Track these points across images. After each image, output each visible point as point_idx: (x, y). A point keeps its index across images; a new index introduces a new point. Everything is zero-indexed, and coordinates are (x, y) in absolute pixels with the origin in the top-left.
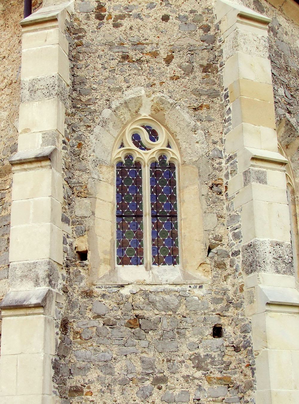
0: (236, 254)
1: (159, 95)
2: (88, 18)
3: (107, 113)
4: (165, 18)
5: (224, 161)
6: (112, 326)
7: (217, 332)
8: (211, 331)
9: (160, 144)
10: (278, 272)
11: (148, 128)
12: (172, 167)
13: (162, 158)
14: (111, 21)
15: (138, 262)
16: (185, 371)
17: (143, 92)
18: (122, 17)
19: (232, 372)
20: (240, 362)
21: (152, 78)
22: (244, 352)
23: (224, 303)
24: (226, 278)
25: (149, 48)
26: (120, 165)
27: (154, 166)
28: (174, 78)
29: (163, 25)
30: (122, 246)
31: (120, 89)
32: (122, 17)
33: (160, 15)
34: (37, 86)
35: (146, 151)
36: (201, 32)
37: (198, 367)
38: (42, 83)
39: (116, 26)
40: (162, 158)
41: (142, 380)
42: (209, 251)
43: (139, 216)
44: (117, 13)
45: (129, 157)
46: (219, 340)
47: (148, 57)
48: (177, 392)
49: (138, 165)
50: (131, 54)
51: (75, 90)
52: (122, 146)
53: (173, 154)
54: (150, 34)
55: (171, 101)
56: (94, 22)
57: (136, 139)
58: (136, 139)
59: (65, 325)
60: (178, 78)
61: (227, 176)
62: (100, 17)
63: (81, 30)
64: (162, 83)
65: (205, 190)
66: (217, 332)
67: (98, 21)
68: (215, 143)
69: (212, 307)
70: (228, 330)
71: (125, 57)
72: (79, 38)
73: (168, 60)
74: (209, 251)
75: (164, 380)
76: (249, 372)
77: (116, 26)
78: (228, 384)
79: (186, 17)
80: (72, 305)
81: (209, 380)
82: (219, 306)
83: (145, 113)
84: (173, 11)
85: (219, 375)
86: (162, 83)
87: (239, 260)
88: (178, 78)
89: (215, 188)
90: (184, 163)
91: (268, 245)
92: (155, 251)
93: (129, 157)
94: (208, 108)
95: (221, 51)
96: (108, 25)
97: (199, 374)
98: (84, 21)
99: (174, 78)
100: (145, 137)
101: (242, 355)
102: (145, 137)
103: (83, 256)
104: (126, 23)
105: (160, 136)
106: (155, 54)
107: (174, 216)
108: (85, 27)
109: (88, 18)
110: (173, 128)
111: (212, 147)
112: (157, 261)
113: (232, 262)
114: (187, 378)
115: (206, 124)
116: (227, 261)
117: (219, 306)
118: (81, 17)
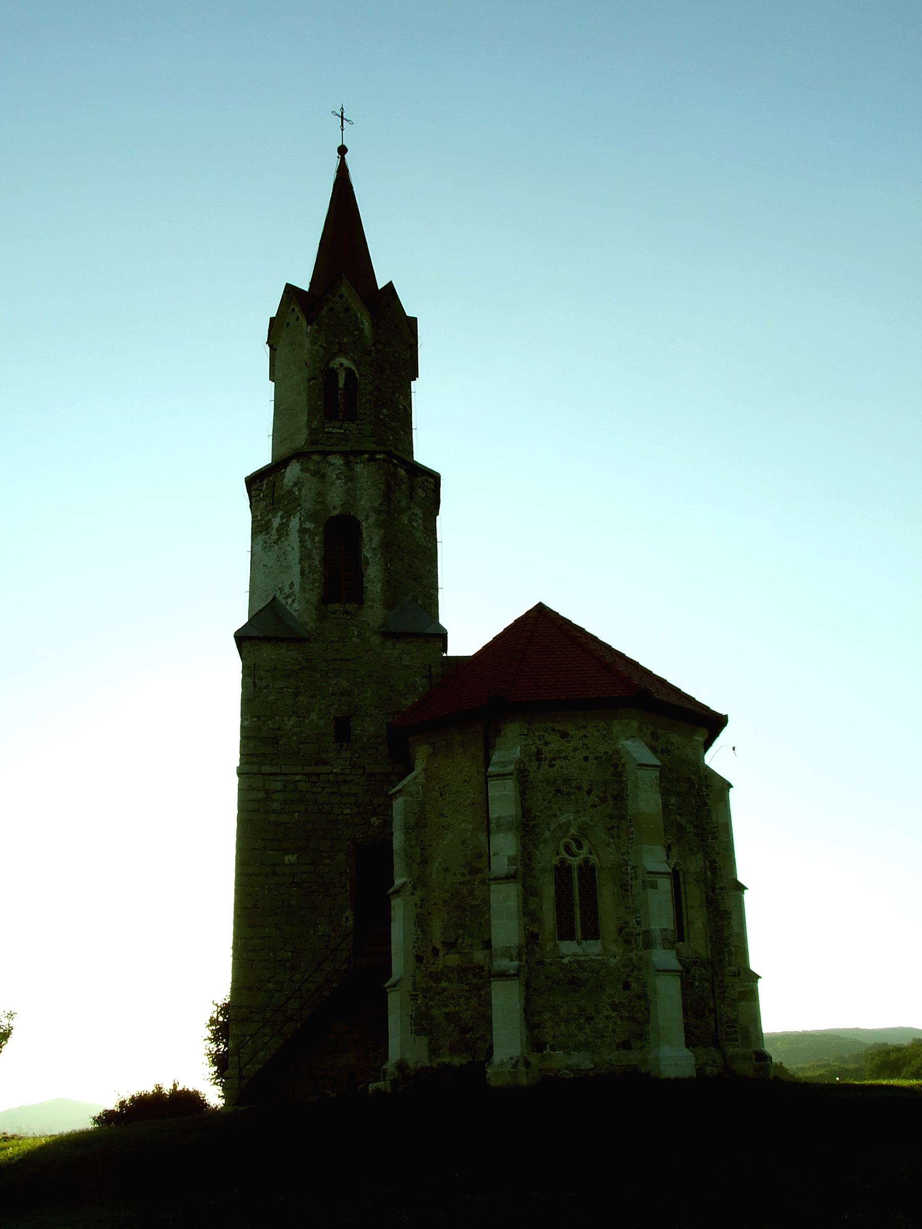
0: (638, 934)
2: (530, 761)
4: (586, 759)
7: (627, 986)
9: (585, 850)
10: (665, 949)
11: (576, 841)
13: (586, 861)
14: (547, 762)
15: (571, 937)
16: (605, 1013)
25: (574, 783)
28: (594, 806)
31: (555, 816)
33: (581, 757)
36: (612, 768)
37: (615, 1010)
39: (551, 766)
42: (621, 931)
44: (551, 756)
46: (627, 992)
47: (574, 790)
48: (601, 1026)
50: (563, 788)
53: (594, 859)
56: (535, 764)
57: (567, 848)
58: (567, 848)
61: (631, 879)
62: (539, 760)
63: (526, 770)
68: (623, 854)
69: (622, 970)
71: (559, 791)
72: (525, 776)
73: (589, 792)
74: (621, 931)
75: (592, 1018)
76: (646, 1013)
77: (551, 766)
78: (632, 1019)
79: (601, 758)
81: (621, 1018)
83: (573, 831)
87: (640, 939)
88: (596, 806)
93: (563, 861)
94: (618, 827)
96: (545, 765)
97: (614, 1014)
98: (528, 764)
99: (594, 806)
106: (579, 788)
109: (530, 761)
112: (585, 937)
114: (607, 1017)
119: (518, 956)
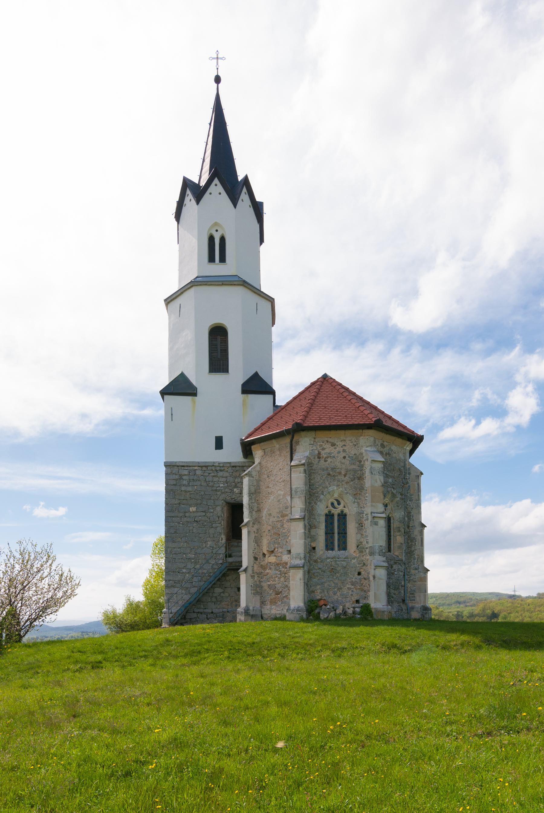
0: (367, 548)
1: (341, 489)
2: (314, 458)
3: (322, 497)
4: (344, 457)
5: (364, 515)
6: (324, 572)
7: (359, 574)
8: (357, 573)
9: (342, 505)
10: (380, 555)
11: (337, 500)
12: (346, 515)
13: (342, 511)
14: (323, 459)
15: (332, 549)
16: (348, 586)
17: (335, 488)
18: (327, 457)
19: (202, 606)
20: (366, 583)
21: (339, 483)
22: (367, 580)
23: (362, 565)
24: (363, 556)
25: (338, 470)
26: (326, 515)
27: (339, 515)
28: (347, 483)
29: (343, 461)
30: (327, 546)
31: (327, 487)
32: (327, 457)
33: (342, 456)
34: (297, 490)
35: (335, 509)
36: (358, 463)
37: (352, 585)
38: (299, 489)
39: (325, 461)
40: (342, 511)
41: (334, 589)
42: (358, 547)
43: (333, 533)
44: (326, 456)
45: (330, 512)
46: (360, 577)
47: (337, 474)
48: (345, 592)
49: (333, 515)
50: (331, 473)
51: (310, 488)
52: (327, 507)
53: (346, 511)
54: (338, 465)
55: (346, 492)
56: (317, 460)
57: (332, 504)
58: (332, 504)
59: (309, 572)
60: (348, 482)
61: (365, 520)
62: (319, 458)
63: (312, 463)
64: (342, 485)
65: (357, 525)
66: (359, 574)
67: (318, 459)
68: (361, 508)
69: (358, 565)
70: (363, 573)
71: (329, 474)
72: (311, 467)
73: (345, 476)
74: (358, 547)
75: (341, 588)
76: (368, 586)
77: (325, 461)
78: (362, 590)
79: (352, 457)
80: (311, 565)
81: (356, 589)
82: (360, 566)
83: (336, 495)
84: (347, 455)
85: (359, 587)
86: (342, 485)
87: (368, 551)
88: (348, 482)
89: (361, 524)
90: (350, 514)
91: (377, 547)
92: (339, 546)
93: (330, 512)
94: (360, 494)
95: (365, 472)
96: (322, 461)
97: (352, 587)
98: (313, 460)
99: (347, 483)
100: (336, 503)
101: (367, 581)
102: (336, 503)
103: (314, 548)
104: (329, 460)
105: (341, 503)
106: (340, 473)
107: (346, 533)
108: (313, 462)
109: (314, 458)
110: (346, 501)
111: (360, 509)
112: (339, 550)
113: (365, 551)
114: (348, 588)
115: (359, 501)
116: (364, 550)
117: (360, 566)
118: (312, 458)
119: (304, 557)
